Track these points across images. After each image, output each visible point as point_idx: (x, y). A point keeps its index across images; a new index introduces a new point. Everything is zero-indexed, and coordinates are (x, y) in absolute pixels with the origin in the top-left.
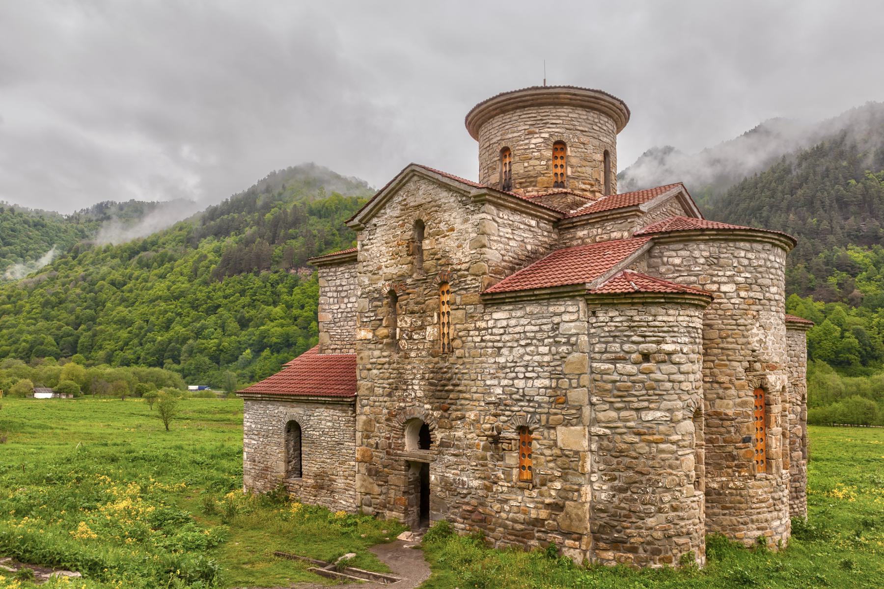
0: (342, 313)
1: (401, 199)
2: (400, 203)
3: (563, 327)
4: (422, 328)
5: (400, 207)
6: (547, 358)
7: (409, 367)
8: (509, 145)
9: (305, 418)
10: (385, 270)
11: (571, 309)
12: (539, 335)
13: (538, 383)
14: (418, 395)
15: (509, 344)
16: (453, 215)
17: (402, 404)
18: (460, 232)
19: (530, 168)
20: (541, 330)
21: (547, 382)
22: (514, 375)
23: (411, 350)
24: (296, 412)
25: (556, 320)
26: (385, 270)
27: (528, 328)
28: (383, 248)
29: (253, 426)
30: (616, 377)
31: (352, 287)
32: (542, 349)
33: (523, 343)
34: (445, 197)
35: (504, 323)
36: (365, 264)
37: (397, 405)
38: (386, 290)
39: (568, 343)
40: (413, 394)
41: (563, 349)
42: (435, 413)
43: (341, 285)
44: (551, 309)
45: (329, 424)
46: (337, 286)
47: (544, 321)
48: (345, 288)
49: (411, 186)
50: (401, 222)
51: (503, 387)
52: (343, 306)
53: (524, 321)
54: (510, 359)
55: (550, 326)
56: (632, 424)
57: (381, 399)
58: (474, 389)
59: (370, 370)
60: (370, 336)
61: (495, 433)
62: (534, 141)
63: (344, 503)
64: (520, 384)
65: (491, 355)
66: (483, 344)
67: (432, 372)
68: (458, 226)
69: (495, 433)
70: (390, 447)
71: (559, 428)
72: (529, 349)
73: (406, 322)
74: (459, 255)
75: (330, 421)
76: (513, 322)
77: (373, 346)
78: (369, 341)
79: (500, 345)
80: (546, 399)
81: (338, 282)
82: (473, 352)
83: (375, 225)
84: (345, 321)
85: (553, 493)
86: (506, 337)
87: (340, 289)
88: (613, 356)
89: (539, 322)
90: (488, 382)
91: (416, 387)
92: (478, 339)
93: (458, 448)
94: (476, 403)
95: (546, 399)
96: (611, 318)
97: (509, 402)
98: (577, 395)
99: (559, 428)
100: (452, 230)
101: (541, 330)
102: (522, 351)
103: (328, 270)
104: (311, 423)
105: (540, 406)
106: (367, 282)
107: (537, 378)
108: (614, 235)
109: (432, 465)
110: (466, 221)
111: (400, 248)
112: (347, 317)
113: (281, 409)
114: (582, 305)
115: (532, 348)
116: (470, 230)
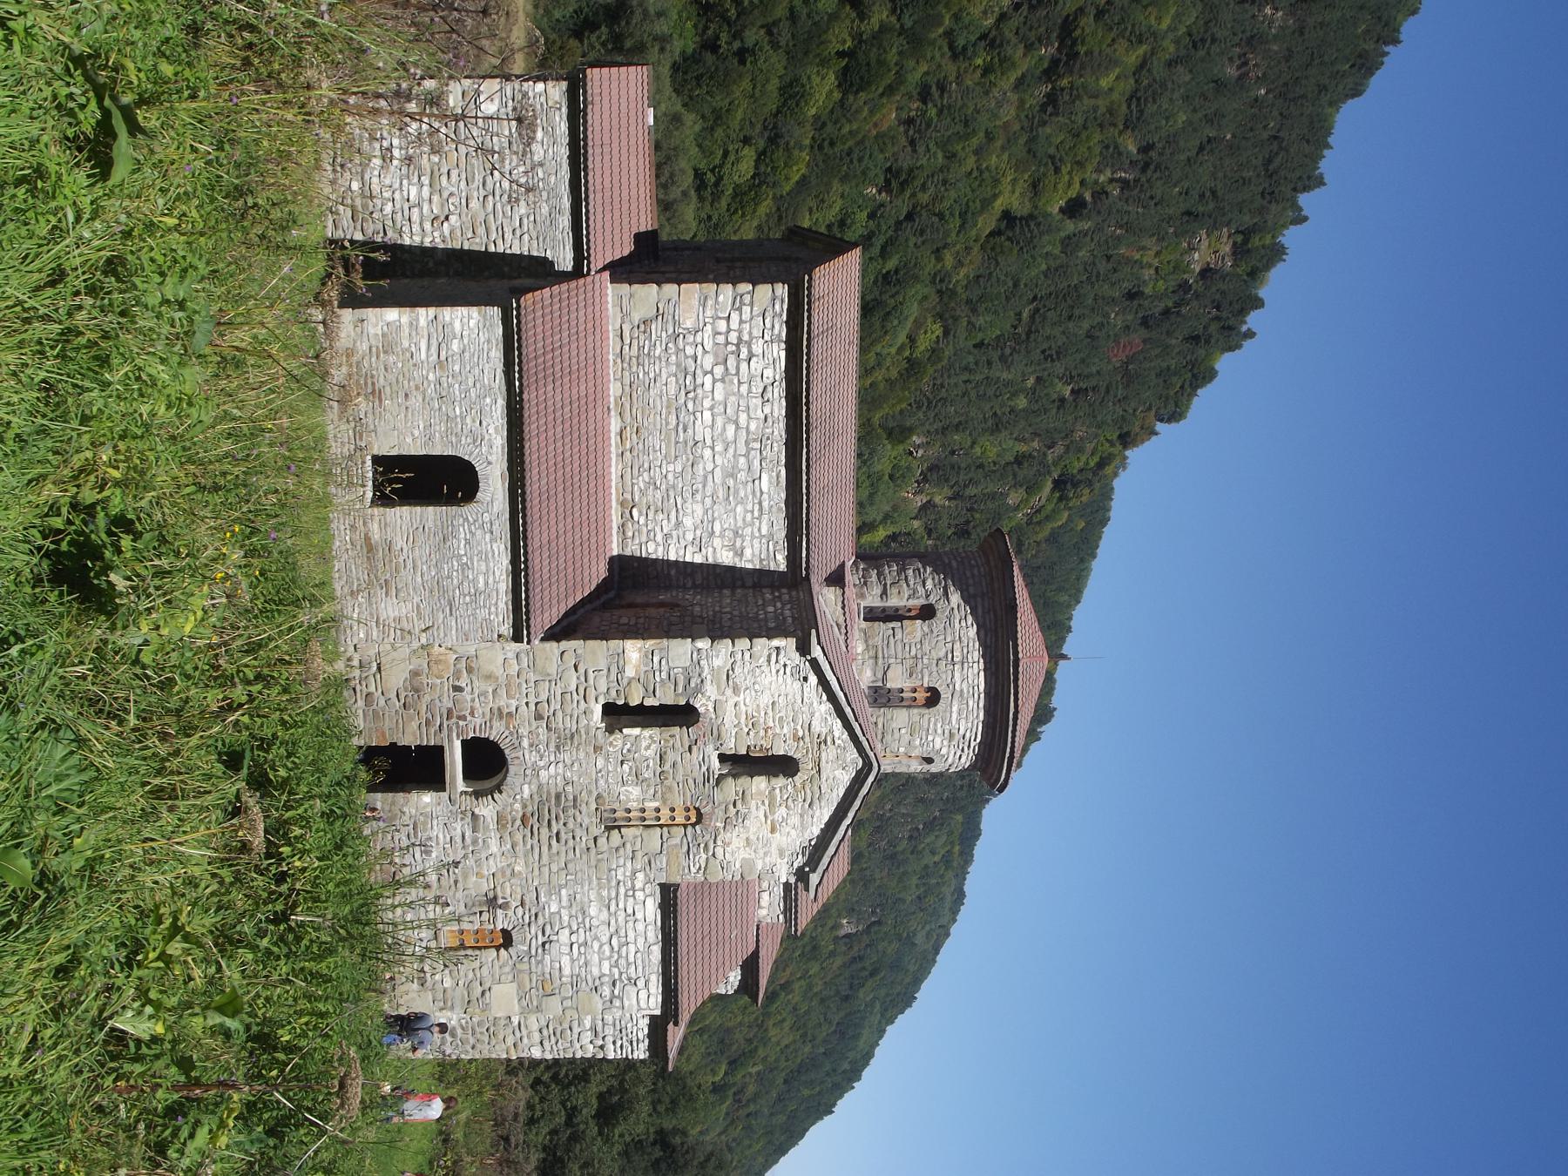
1: (837, 734)
2: (831, 731)
3: (631, 990)
5: (824, 731)
6: (596, 972)
7: (582, 755)
8: (941, 706)
9: (486, 517)
10: (731, 703)
11: (652, 1000)
12: (622, 962)
13: (565, 960)
14: (543, 773)
15: (613, 922)
16: (793, 832)
17: (525, 743)
18: (767, 843)
19: (897, 735)
20: (629, 964)
21: (567, 971)
22: (575, 928)
23: (607, 760)
25: (641, 983)
26: (731, 703)
27: (632, 948)
28: (765, 700)
30: (576, 1030)
31: (744, 388)
32: (606, 964)
33: (615, 942)
34: (824, 814)
35: (639, 915)
36: (747, 655)
37: (524, 731)
39: (613, 996)
40: (542, 764)
41: (606, 991)
42: (518, 806)
44: (654, 978)
46: (749, 344)
47: (640, 969)
48: (744, 366)
49: (852, 754)
50: (800, 734)
51: (559, 913)
52: (708, 362)
53: (641, 941)
54: (595, 922)
55: (634, 976)
56: (525, 1040)
58: (554, 868)
59: (576, 667)
60: (630, 672)
61: (500, 901)
62: (938, 740)
64: (564, 936)
65: (599, 894)
66: (614, 883)
67: (575, 799)
68: (779, 839)
69: (500, 901)
70: (459, 718)
71: (514, 985)
72: (606, 948)
73: (648, 748)
75: (487, 583)
76: (640, 926)
77: (613, 677)
78: (621, 671)
79: (613, 908)
80: (547, 970)
81: (757, 348)
82: (604, 866)
83: (805, 679)
84: (678, 365)
85: (438, 977)
86: (621, 915)
88: (599, 1028)
89: (639, 962)
90: (564, 892)
92: (620, 877)
93: (475, 842)
94: (536, 872)
95: (547, 970)
97: (541, 921)
98: (554, 1006)
99: (514, 985)
100: (773, 830)
101: (629, 964)
102: (605, 939)
104: (479, 532)
105: (538, 963)
106: (717, 662)
107: (573, 961)
108: (765, 896)
109: (444, 795)
110: (781, 854)
111: (762, 733)
114: (658, 1012)
115: (607, 953)
116: (767, 859)
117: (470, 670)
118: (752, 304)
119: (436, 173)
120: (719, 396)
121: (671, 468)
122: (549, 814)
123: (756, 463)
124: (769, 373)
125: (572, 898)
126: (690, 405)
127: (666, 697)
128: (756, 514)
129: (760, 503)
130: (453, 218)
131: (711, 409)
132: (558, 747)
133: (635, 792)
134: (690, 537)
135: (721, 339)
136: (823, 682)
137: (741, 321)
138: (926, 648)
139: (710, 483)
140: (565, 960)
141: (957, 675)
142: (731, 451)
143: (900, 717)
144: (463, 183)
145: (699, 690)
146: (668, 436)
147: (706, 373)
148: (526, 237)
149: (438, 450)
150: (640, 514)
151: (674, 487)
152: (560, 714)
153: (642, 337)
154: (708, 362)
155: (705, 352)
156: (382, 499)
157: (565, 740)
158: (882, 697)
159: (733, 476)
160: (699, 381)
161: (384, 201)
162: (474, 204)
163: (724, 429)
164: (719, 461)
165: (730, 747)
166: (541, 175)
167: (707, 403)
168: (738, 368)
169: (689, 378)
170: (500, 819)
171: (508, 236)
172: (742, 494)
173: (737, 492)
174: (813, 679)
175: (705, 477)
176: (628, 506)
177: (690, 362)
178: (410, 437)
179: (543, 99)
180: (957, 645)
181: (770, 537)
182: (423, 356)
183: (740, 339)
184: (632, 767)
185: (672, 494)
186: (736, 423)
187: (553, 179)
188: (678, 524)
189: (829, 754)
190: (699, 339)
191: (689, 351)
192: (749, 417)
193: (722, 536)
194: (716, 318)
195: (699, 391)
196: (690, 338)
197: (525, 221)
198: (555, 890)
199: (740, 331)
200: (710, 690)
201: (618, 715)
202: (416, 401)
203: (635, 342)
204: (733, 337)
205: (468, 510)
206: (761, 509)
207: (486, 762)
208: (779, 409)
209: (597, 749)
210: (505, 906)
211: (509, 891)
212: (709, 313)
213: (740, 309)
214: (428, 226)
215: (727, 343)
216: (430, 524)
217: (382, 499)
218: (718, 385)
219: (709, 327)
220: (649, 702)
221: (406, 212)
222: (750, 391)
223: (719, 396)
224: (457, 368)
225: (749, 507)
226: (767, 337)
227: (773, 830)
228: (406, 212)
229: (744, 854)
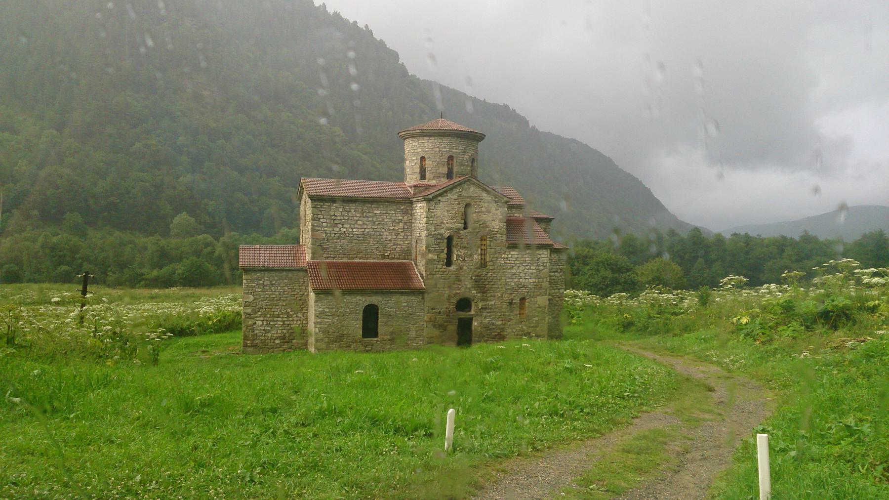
4: (471, 255)
13: (531, 280)
24: (374, 300)
28: (446, 214)
34: (485, 195)
38: (447, 235)
49: (465, 186)
52: (336, 229)
60: (436, 257)
74: (493, 224)
78: (434, 260)
96: (555, 257)
106: (433, 229)
113: (358, 298)
122: (481, 285)
125: (509, 278)
127: (444, 245)
133: (475, 256)
136: (440, 195)
140: (531, 280)
143: (455, 169)
145: (442, 235)
149: (361, 317)
156: (375, 335)
157: (458, 279)
158: (450, 175)
165: (461, 226)
170: (482, 300)
174: (440, 198)
176: (384, 257)
178: (356, 327)
181: (395, 210)
184: (466, 259)
188: (390, 240)
189: (464, 193)
194: (322, 226)
198: (507, 284)
200: (442, 231)
201: (449, 263)
202: (345, 323)
205: (381, 308)
207: (464, 304)
208: (353, 206)
209: (461, 268)
210: (512, 300)
211: (506, 298)
216: (385, 320)
217: (375, 335)
220: (445, 251)
227: (490, 212)
229: (497, 222)
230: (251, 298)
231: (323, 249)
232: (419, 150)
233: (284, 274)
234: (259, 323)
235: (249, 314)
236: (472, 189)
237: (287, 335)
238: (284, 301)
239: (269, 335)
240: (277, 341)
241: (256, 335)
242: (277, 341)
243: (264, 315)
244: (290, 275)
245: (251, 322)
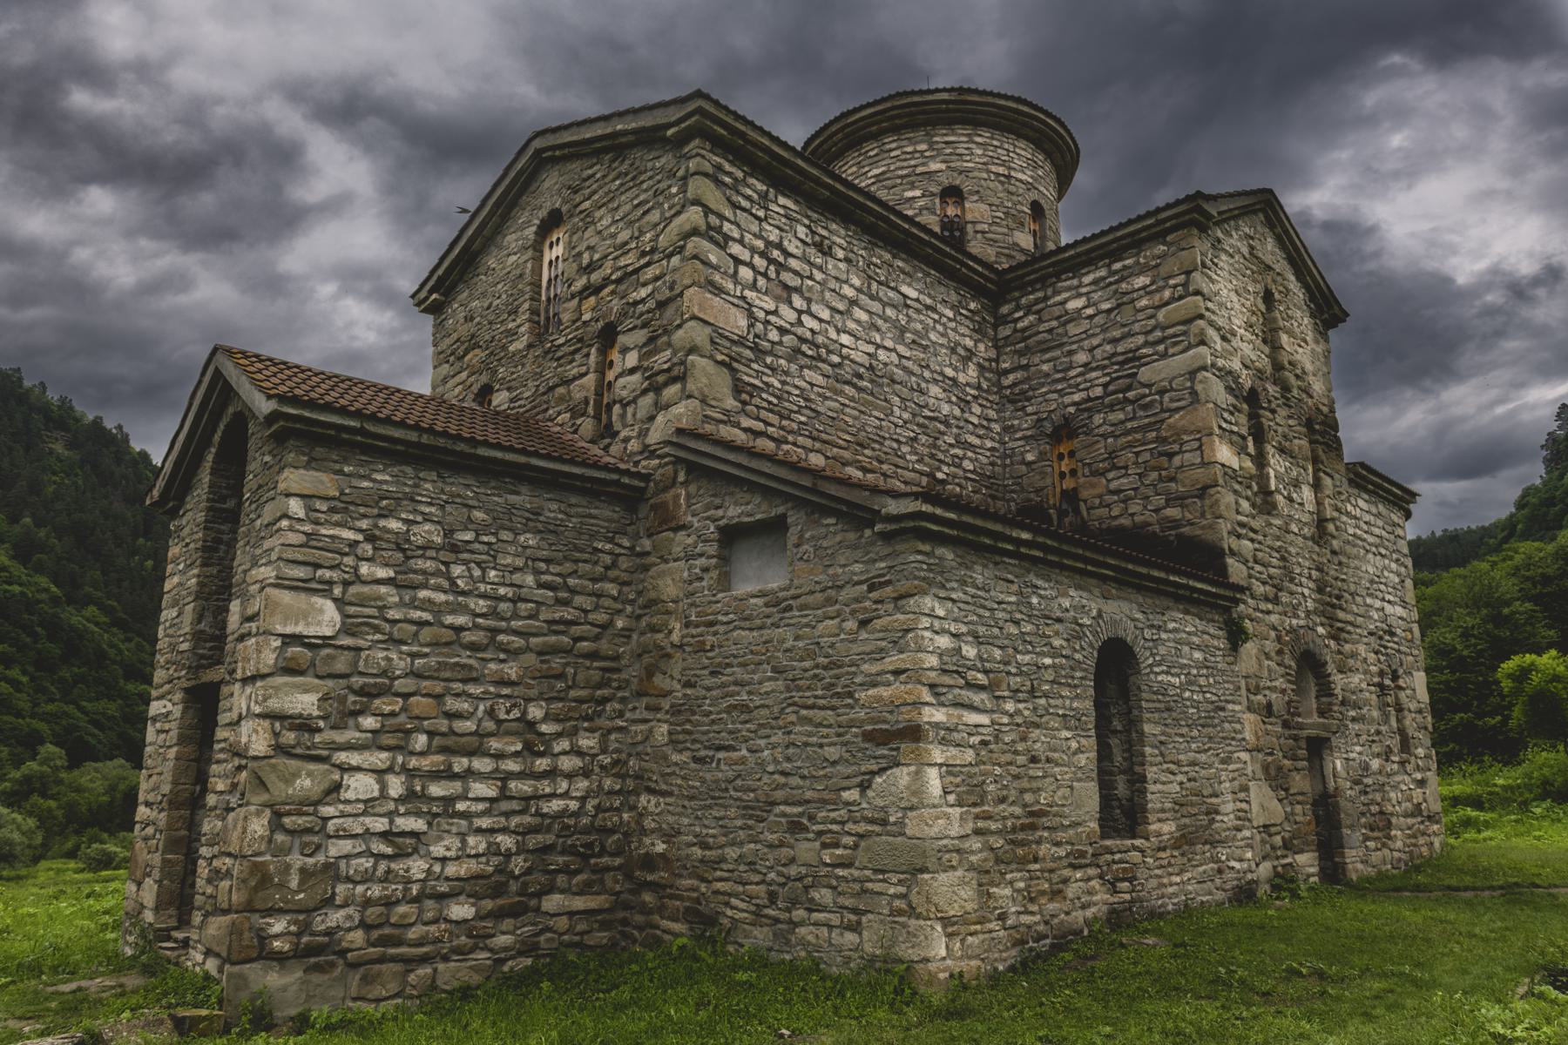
0: (783, 331)
4: (1296, 484)
9: (1148, 634)
24: (1122, 614)
29: (970, 651)
43: (779, 246)
45: (1198, 655)
46: (768, 243)
48: (793, 263)
52: (789, 315)
57: (1263, 606)
63: (1237, 865)
75: (1198, 648)
81: (774, 236)
87: (776, 253)
91: (1306, 592)
103: (740, 175)
112: (798, 351)
117: (1258, 690)
118: (722, 217)
119: (450, 741)
120: (825, 314)
121: (897, 411)
123: (891, 294)
124: (802, 231)
126: (836, 359)
128: (936, 317)
129: (928, 307)
130: (535, 712)
131: (838, 331)
132: (1292, 580)
134: (957, 412)
135: (761, 282)
137: (741, 242)
138: (997, 202)
139: (909, 364)
141: (1020, 176)
142: (880, 322)
144: (475, 690)
146: (866, 403)
147: (800, 323)
148: (571, 581)
150: (939, 469)
151: (914, 415)
152: (1272, 571)
153: (756, 401)
154: (789, 315)
155: (775, 313)
159: (903, 330)
160: (808, 335)
161: (493, 849)
162: (512, 671)
163: (858, 322)
164: (889, 343)
166: (469, 536)
167: (833, 335)
168: (796, 273)
169: (804, 348)
171: (568, 614)
172: (919, 327)
173: (916, 332)
175: (905, 369)
177: (786, 339)
179: (319, 505)
180: (993, 168)
182: (984, 719)
183: (763, 254)
185: (922, 420)
186: (853, 303)
187: (478, 515)
190: (761, 315)
191: (774, 335)
192: (846, 282)
193: (955, 369)
195: (820, 339)
196: (759, 326)
197: (545, 578)
199: (753, 250)
200: (1236, 365)
203: (763, 414)
204: (759, 262)
206: (934, 310)
212: (730, 286)
213: (727, 238)
214: (542, 764)
215: (765, 275)
218: (815, 308)
219: (747, 293)
221: (515, 805)
222: (820, 268)
223: (825, 314)
224: (997, 653)
225: (931, 322)
226: (761, 213)
228: (515, 805)
230: (325, 618)
231: (738, 388)
232: (935, 166)
233: (523, 499)
234: (360, 786)
235: (303, 725)
236: (1270, 244)
237: (518, 864)
238: (514, 653)
239: (417, 867)
240: (461, 910)
241: (331, 871)
242: (461, 910)
243: (393, 737)
244: (552, 510)
245: (306, 782)
